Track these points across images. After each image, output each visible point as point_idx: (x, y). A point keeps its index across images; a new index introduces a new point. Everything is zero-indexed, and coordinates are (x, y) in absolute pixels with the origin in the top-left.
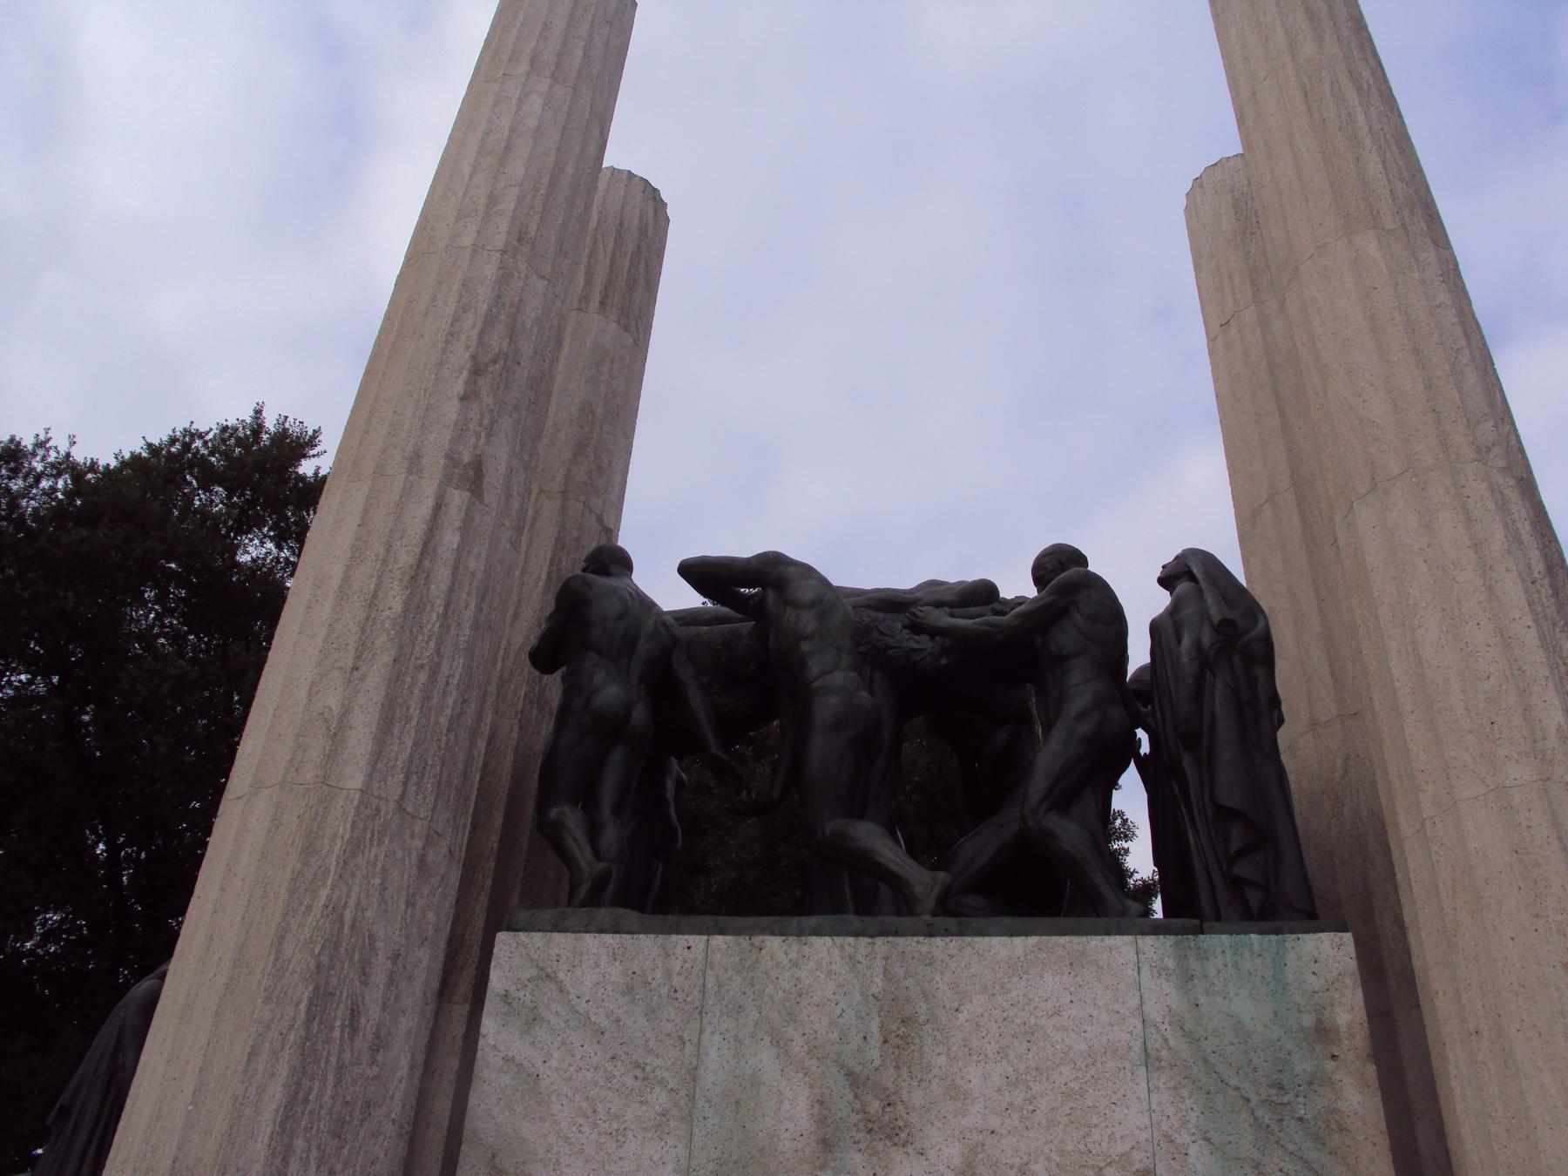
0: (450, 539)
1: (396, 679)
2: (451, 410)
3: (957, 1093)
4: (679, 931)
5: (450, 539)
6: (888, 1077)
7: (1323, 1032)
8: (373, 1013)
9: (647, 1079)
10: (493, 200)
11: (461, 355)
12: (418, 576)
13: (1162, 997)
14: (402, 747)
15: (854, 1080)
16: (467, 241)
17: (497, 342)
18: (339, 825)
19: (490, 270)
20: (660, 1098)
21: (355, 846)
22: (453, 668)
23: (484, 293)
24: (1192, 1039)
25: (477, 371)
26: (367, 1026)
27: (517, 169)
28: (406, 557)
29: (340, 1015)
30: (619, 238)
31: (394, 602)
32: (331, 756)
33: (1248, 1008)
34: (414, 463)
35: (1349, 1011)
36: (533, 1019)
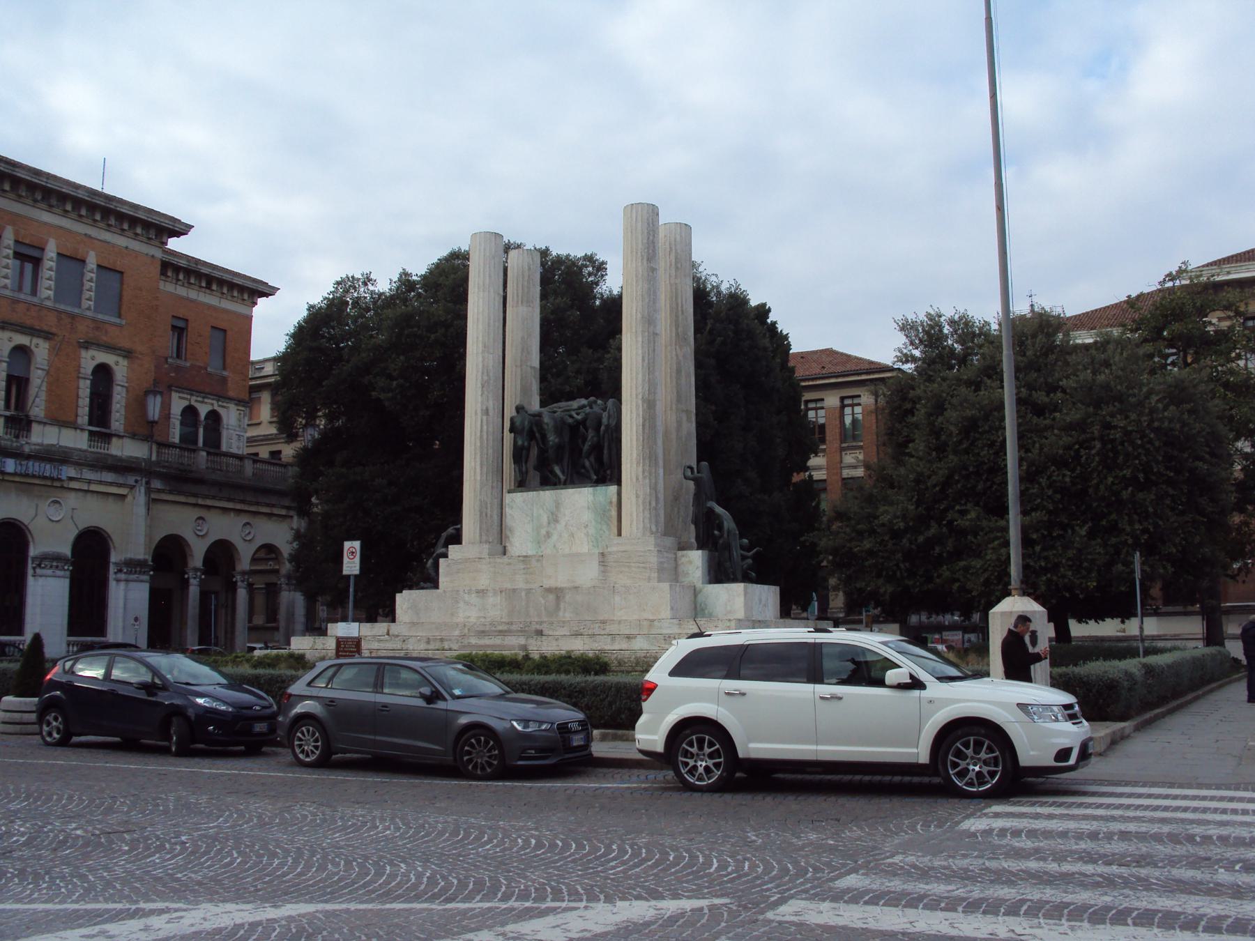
0: (485, 427)
1: (481, 457)
2: (480, 399)
3: (565, 515)
5: (485, 427)
7: (611, 503)
8: (489, 513)
9: (527, 515)
10: (477, 338)
11: (479, 385)
12: (481, 437)
13: (591, 498)
14: (485, 469)
15: (552, 513)
16: (475, 352)
17: (485, 378)
18: (478, 486)
19: (480, 359)
20: (529, 519)
21: (481, 489)
22: (490, 451)
23: (480, 366)
25: (483, 387)
26: (489, 515)
27: (480, 327)
28: (478, 434)
29: (484, 514)
30: (523, 275)
31: (478, 444)
32: (475, 473)
34: (476, 413)
35: (615, 499)
36: (512, 508)
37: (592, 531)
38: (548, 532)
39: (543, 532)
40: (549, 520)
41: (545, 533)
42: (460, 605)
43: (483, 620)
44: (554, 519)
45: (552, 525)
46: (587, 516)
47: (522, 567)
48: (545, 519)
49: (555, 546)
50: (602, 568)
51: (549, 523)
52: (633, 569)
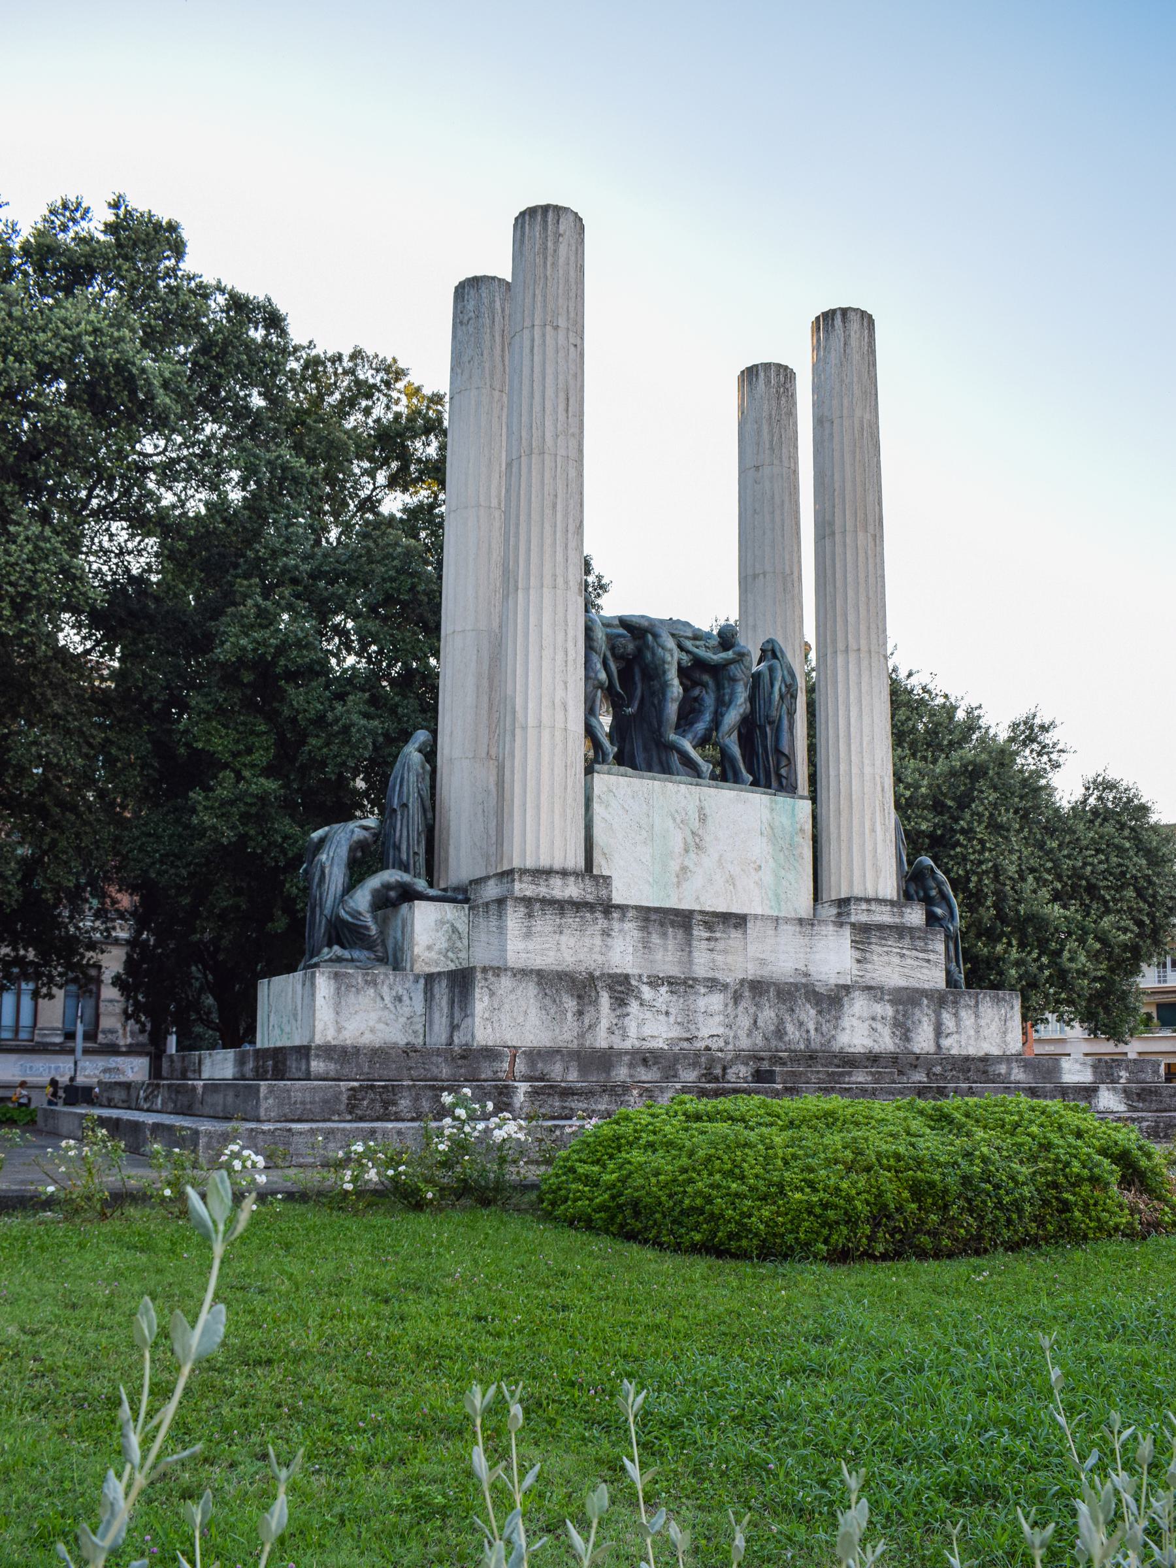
3: (717, 839)
4: (643, 778)
6: (700, 832)
13: (766, 814)
15: (693, 833)
24: (772, 829)
33: (786, 822)
37: (767, 877)
38: (684, 869)
39: (674, 866)
40: (686, 843)
41: (678, 868)
42: (629, 1009)
43: (685, 1045)
44: (696, 844)
45: (692, 855)
46: (760, 848)
47: (707, 935)
48: (677, 840)
49: (698, 898)
50: (858, 955)
51: (687, 851)
52: (909, 961)
